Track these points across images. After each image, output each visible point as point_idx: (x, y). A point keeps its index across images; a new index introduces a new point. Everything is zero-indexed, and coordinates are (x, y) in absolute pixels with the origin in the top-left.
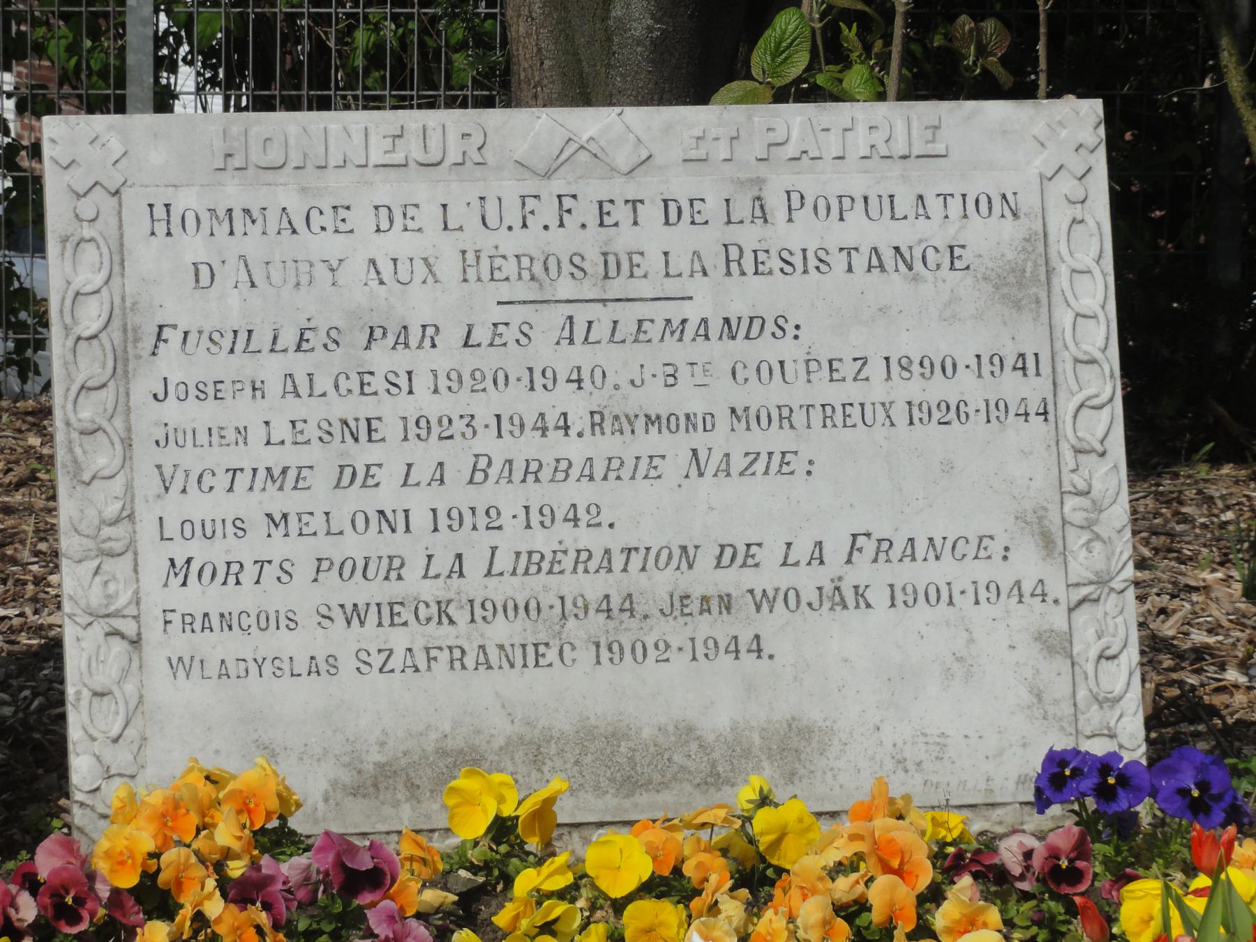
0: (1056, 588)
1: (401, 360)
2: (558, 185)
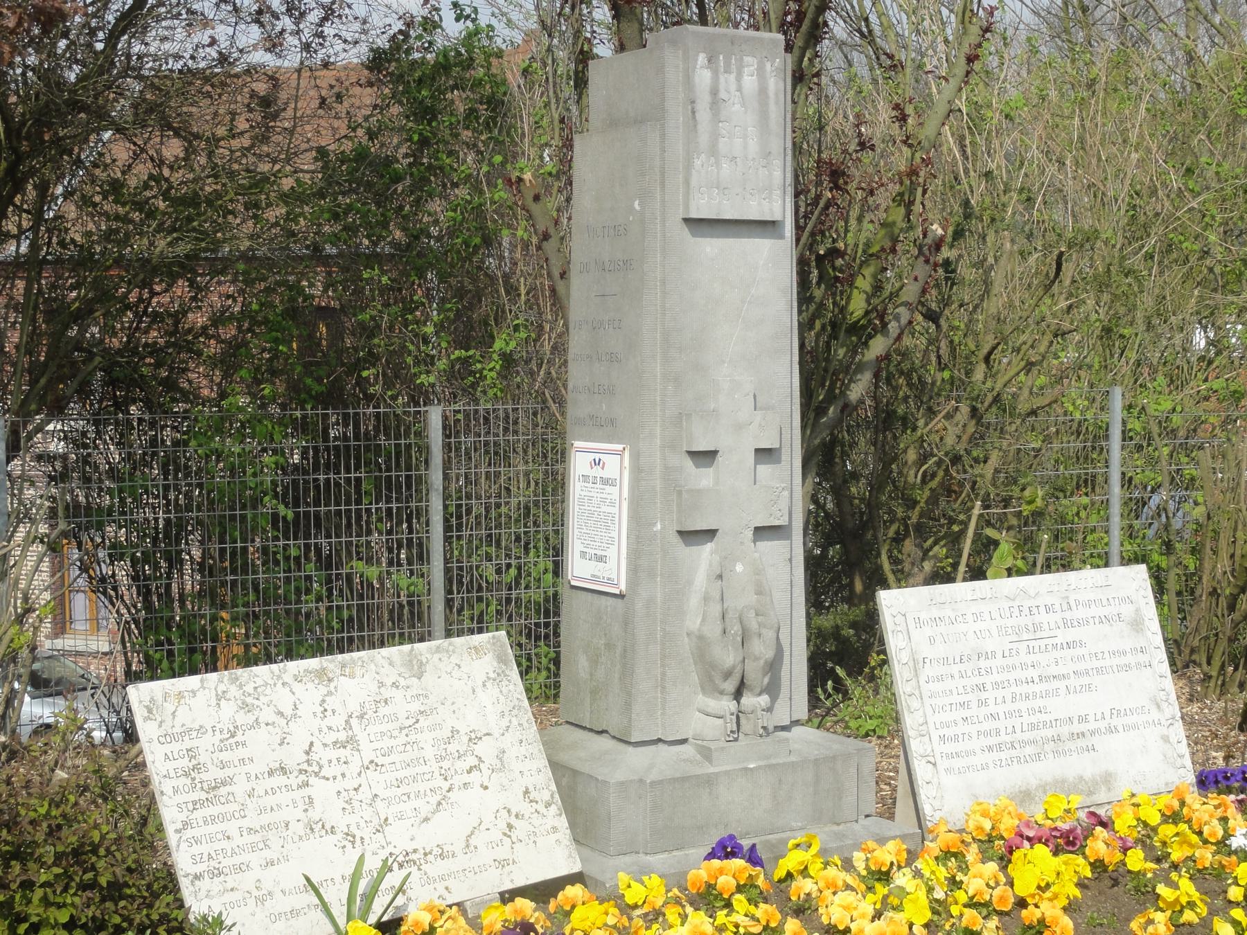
0: (1163, 722)
1: (988, 663)
2: (1017, 603)
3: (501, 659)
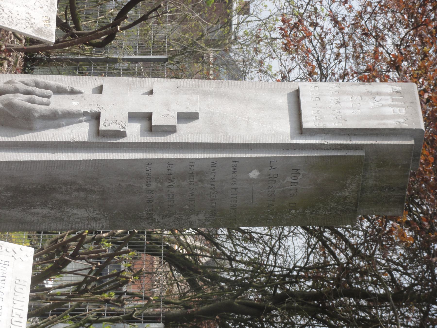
3: (39, 31)
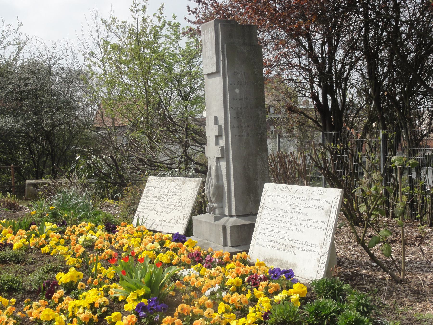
0: (320, 253)
2: (295, 195)
3: (198, 184)
